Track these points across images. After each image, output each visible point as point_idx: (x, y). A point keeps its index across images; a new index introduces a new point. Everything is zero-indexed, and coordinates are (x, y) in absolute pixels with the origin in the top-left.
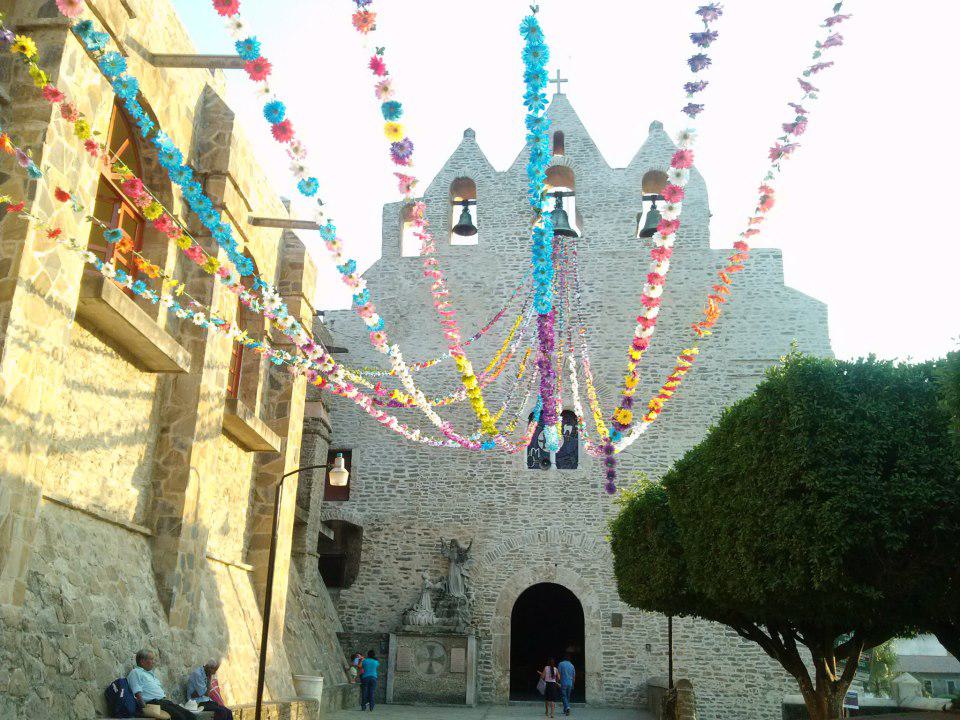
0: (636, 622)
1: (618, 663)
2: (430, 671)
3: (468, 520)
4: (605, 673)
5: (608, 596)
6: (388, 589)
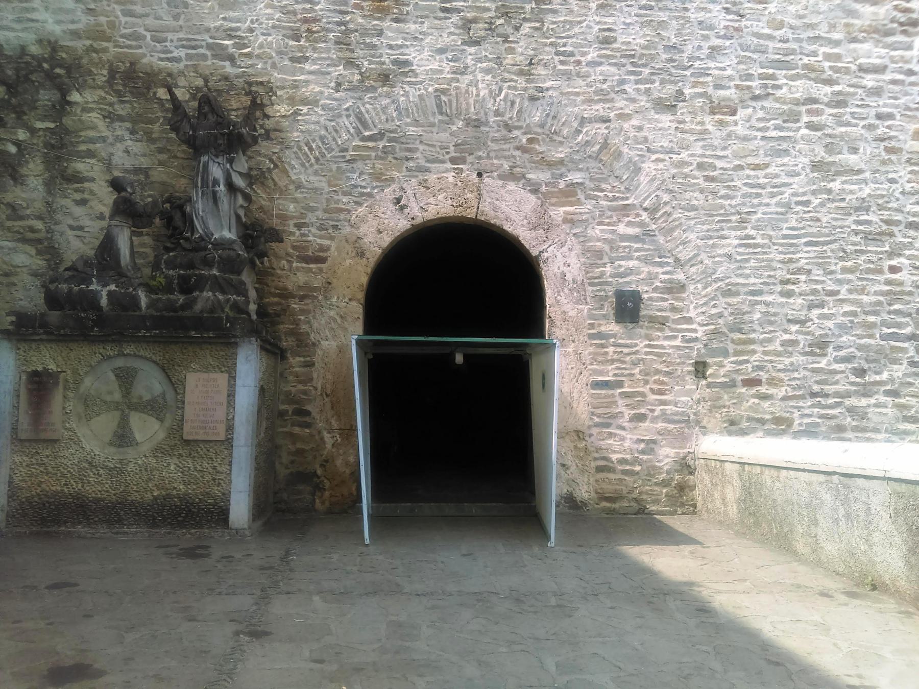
2: (123, 438)
6: (32, 230)
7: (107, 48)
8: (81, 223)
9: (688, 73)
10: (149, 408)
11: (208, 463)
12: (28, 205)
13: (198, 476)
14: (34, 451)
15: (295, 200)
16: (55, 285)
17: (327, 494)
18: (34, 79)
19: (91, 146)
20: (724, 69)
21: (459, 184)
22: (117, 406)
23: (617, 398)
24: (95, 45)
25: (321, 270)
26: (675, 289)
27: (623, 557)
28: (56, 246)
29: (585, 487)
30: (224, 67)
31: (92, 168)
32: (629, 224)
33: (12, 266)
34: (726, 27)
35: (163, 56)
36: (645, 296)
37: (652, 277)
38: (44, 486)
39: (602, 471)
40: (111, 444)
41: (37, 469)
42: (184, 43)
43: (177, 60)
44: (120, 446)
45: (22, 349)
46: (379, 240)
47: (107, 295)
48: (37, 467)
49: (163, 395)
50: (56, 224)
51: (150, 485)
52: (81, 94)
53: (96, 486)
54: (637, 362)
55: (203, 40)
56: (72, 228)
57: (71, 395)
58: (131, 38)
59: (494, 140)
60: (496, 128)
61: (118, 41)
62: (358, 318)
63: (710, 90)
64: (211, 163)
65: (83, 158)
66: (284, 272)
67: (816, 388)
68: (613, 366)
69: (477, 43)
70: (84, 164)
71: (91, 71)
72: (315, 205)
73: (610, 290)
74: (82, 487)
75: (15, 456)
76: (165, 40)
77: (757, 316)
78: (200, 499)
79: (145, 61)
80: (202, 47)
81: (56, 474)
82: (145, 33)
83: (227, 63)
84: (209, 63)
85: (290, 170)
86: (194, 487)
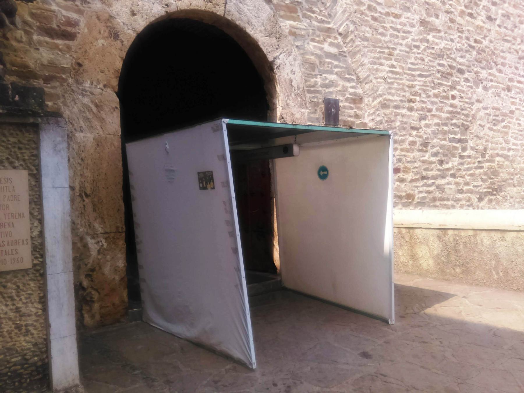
11: (7, 305)
17: (96, 306)
25: (69, 48)
26: (357, 100)
27: (429, 316)
36: (341, 104)
37: (345, 89)
46: (133, 23)
62: (117, 108)
66: (22, 45)
67: (424, 173)
73: (320, 98)
77: (398, 124)
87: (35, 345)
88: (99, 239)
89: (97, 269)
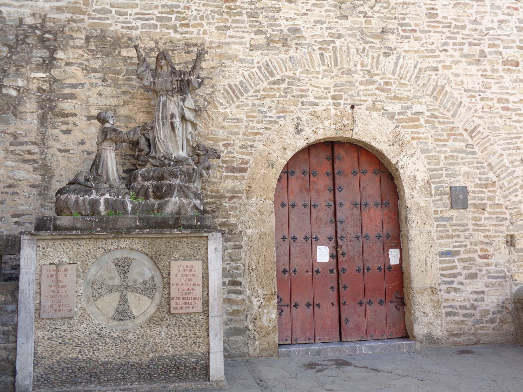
0: (489, 198)
1: (464, 268)
3: (187, 25)
4: (443, 287)
5: (442, 157)
6: (30, 153)
7: (83, 19)
8: (68, 148)
9: (486, 38)
10: (142, 289)
12: (26, 134)
13: (183, 340)
14: (54, 327)
15: (223, 127)
16: (66, 195)
17: (257, 342)
18: (29, 42)
19: (73, 91)
20: (509, 36)
21: (339, 114)
22: (117, 288)
23: (457, 263)
24: (74, 17)
25: (243, 177)
28: (49, 164)
29: (439, 327)
30: (169, 33)
31: (74, 106)
32: (455, 140)
33: (15, 179)
34: (509, 8)
35: (125, 25)
36: (469, 189)
38: (62, 354)
39: (450, 316)
40: (114, 318)
41: (56, 341)
42: (140, 16)
43: (136, 28)
44: (121, 320)
45: (41, 246)
47: (104, 202)
48: (56, 340)
49: (153, 278)
50: (47, 148)
51: (146, 349)
52: (64, 53)
53: (104, 352)
54: (468, 237)
55: (154, 14)
56: (60, 150)
57: (80, 281)
58: (101, 12)
59: (362, 84)
60: (362, 75)
61: (91, 14)
63: (501, 49)
64: (168, 102)
65: (67, 99)
68: (453, 240)
69: (346, 17)
70: (68, 104)
71: (71, 36)
72: (237, 130)
74: (93, 353)
75: (38, 331)
76: (125, 14)
78: (185, 359)
79: (111, 29)
80: (153, 19)
81: (72, 344)
82: (111, 9)
83: (171, 31)
84: (158, 30)
85: (219, 106)
86: (180, 349)
87: (203, 354)
88: (260, 299)
89: (258, 318)
